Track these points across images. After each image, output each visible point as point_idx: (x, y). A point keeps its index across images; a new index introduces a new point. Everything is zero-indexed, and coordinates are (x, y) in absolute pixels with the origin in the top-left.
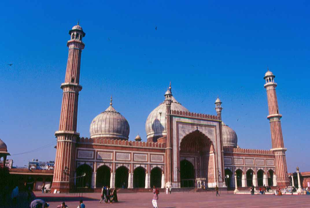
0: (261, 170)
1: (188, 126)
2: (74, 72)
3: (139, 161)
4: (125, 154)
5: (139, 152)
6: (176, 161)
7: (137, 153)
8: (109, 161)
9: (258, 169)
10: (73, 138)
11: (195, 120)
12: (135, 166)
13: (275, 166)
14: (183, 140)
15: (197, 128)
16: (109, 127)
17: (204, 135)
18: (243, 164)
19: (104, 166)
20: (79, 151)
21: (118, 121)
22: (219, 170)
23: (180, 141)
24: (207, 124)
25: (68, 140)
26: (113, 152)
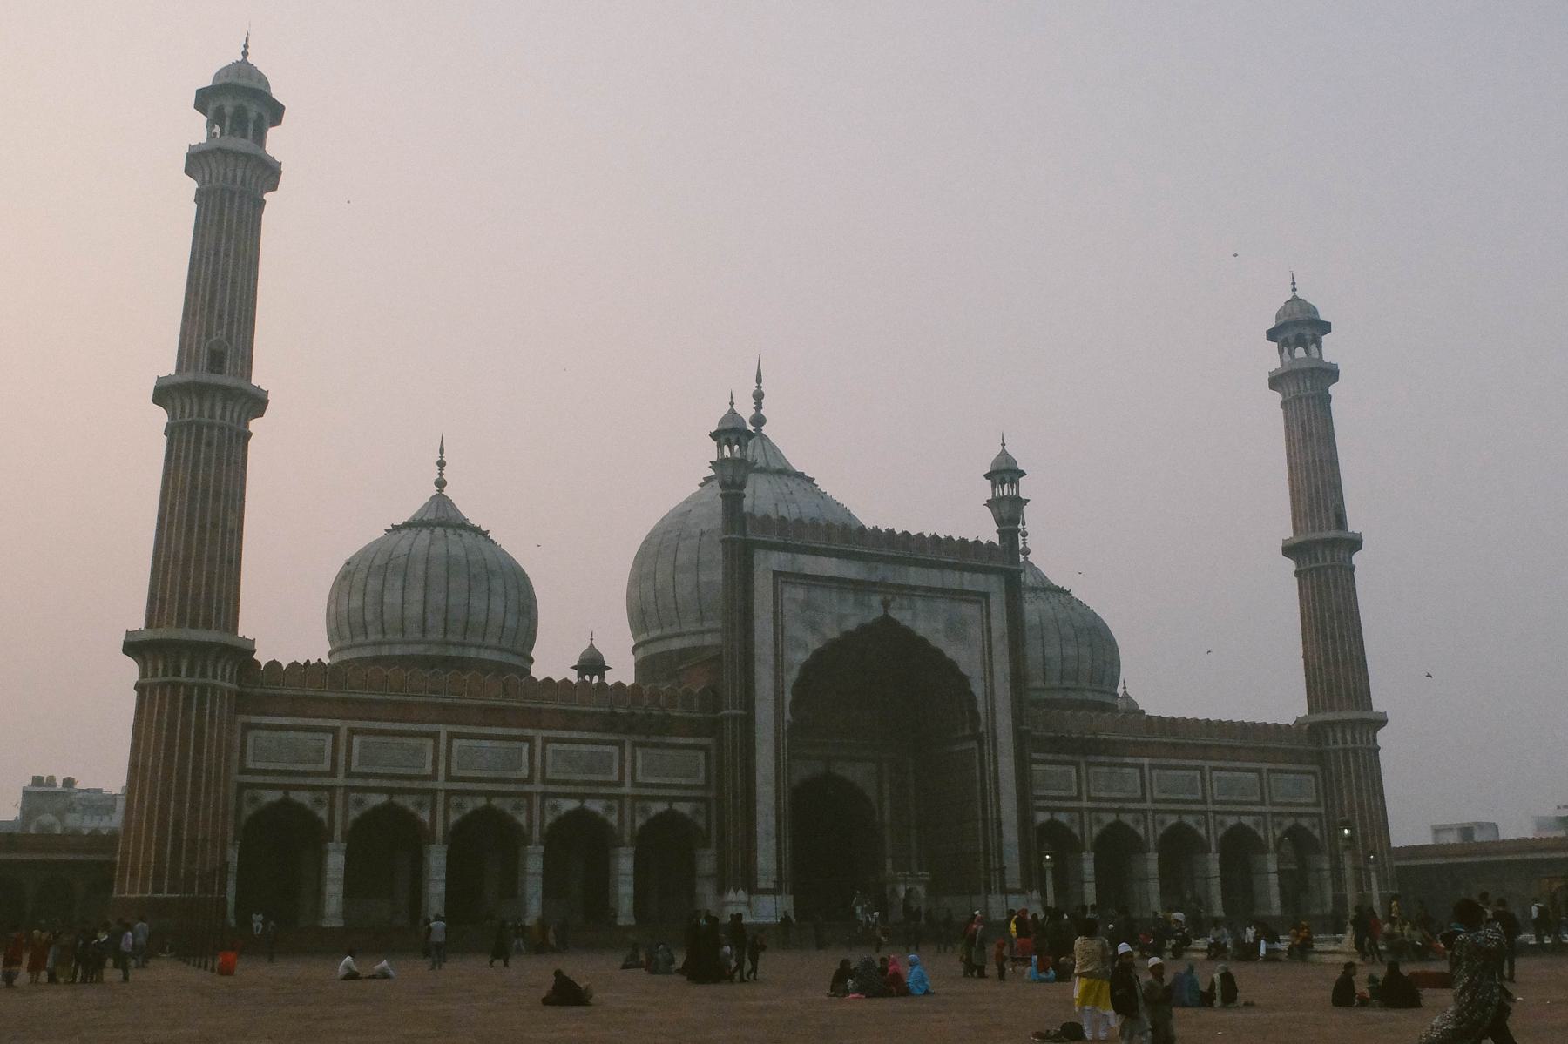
0: (1240, 825)
2: (220, 317)
3: (576, 784)
4: (505, 744)
5: (575, 735)
6: (772, 778)
8: (416, 785)
9: (1222, 823)
12: (554, 807)
13: (1322, 810)
14: (806, 668)
15: (886, 604)
16: (425, 602)
17: (923, 641)
19: (391, 810)
23: (791, 677)
25: (190, 674)
26: (434, 736)
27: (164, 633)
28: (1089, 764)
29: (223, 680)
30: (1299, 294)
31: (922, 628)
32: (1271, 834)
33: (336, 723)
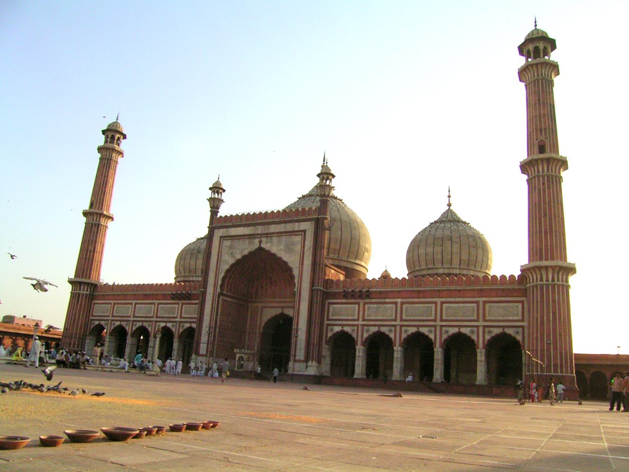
1: (241, 242)
4: (148, 305)
5: (166, 301)
7: (163, 304)
9: (447, 332)
10: (82, 288)
11: (257, 227)
14: (228, 271)
15: (260, 242)
17: (274, 255)
18: (393, 317)
20: (96, 305)
21: (193, 252)
22: (299, 333)
23: (222, 275)
24: (282, 230)
26: (132, 304)
27: (80, 280)
28: (365, 304)
29: (85, 291)
30: (537, 28)
31: (274, 250)
32: (481, 339)
33: (111, 301)
